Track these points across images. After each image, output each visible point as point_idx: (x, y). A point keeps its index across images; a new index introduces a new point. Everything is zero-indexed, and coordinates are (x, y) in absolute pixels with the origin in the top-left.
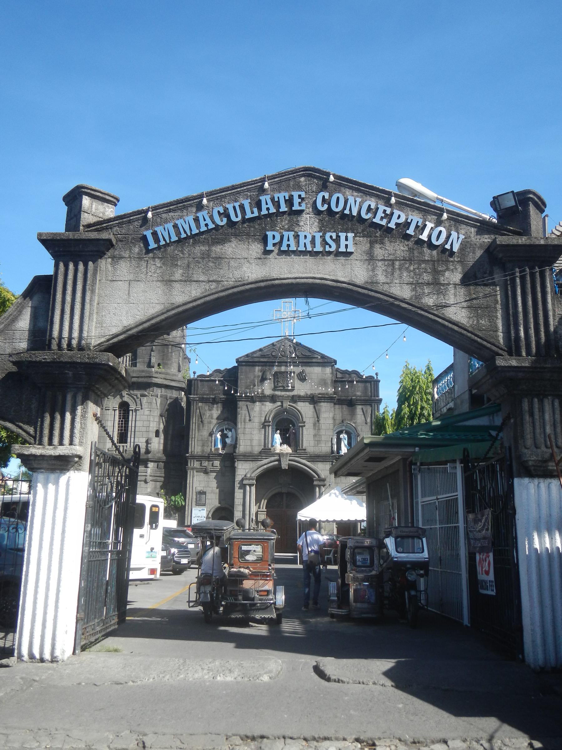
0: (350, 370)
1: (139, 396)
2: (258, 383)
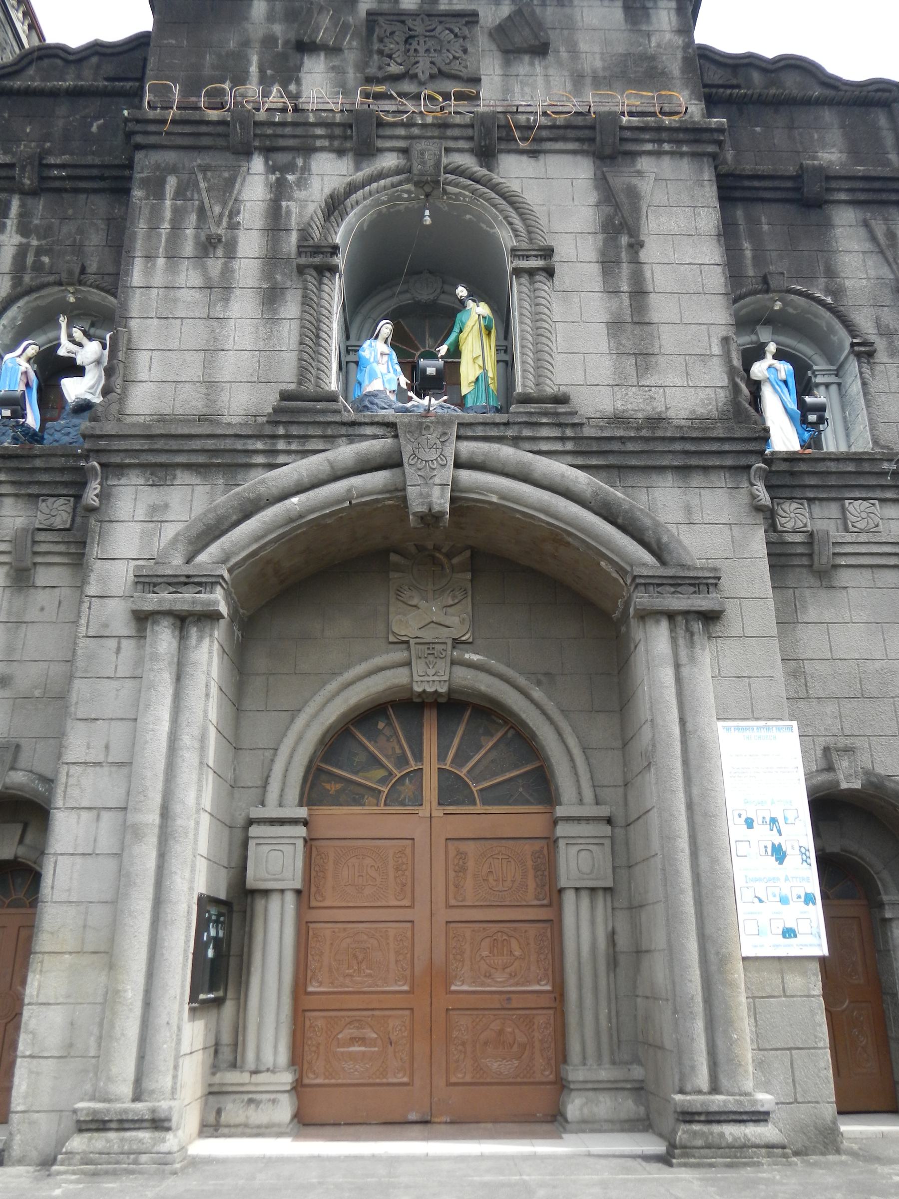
0: (769, 52)
2: (262, 71)
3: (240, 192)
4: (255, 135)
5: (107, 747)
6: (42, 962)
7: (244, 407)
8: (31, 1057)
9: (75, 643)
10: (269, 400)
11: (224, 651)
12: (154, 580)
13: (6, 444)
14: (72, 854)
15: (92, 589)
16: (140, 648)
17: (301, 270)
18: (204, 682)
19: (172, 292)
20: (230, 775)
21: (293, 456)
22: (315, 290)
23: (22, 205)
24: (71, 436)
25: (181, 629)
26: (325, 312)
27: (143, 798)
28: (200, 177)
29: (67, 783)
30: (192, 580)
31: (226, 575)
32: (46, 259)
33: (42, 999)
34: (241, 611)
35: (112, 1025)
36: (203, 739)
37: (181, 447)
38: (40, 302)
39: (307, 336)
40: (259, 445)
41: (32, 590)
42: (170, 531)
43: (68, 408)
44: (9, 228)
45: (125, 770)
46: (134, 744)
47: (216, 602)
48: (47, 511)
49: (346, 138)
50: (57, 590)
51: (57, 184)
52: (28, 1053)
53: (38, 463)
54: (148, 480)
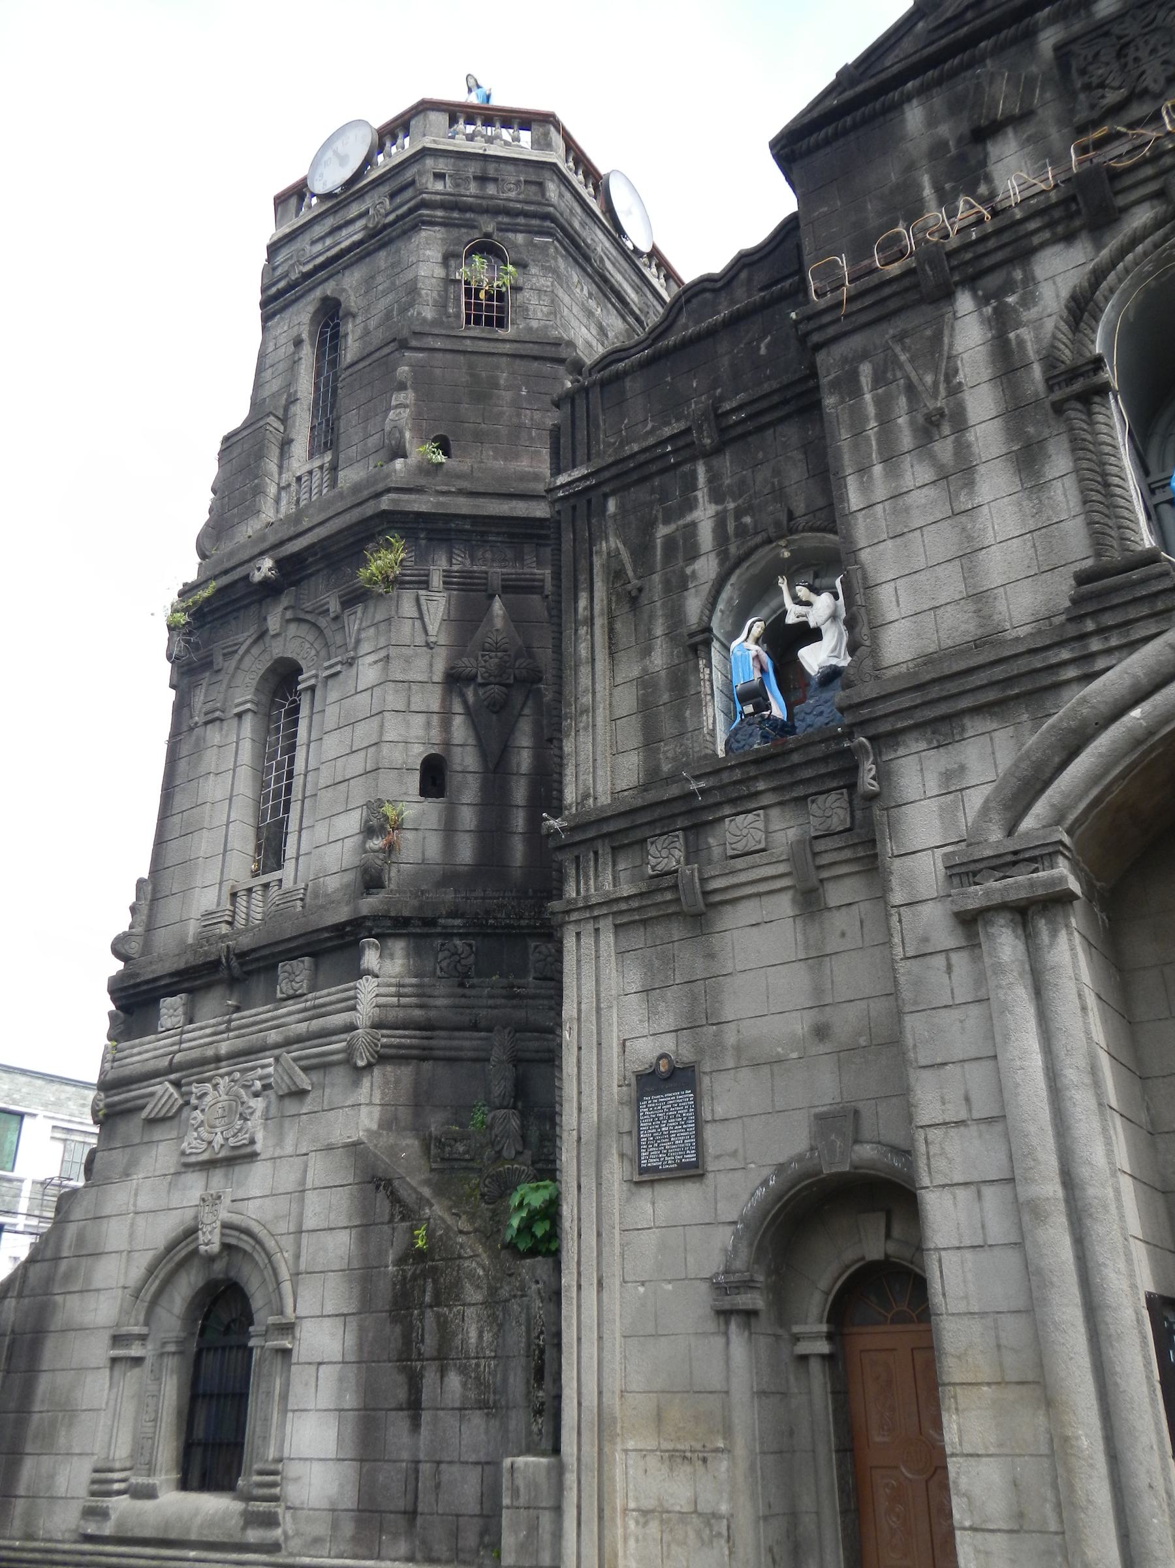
1: (334, 606)
3: (951, 345)
4: (952, 269)
5: (967, 1099)
6: (955, 1397)
7: (1030, 611)
8: (973, 1529)
9: (894, 970)
10: (1062, 589)
11: (1090, 944)
12: (972, 867)
13: (756, 746)
14: (958, 1248)
15: (897, 897)
16: (977, 959)
17: (1058, 408)
18: (1074, 991)
19: (900, 502)
20: (1143, 1118)
21: (1117, 654)
22: (1085, 427)
23: (709, 469)
24: (825, 715)
25: (1025, 926)
26: (1107, 449)
27: (1032, 1163)
28: (898, 349)
29: (928, 1153)
30: (1021, 856)
31: (1066, 839)
32: (747, 520)
33: (968, 1449)
34: (1098, 884)
35: (1071, 1488)
36: (1094, 1070)
37: (961, 689)
38: (752, 571)
39: (1092, 490)
40: (1065, 655)
41: (826, 914)
42: (975, 800)
43: (813, 683)
44: (701, 500)
45: (998, 1128)
46: (1001, 1091)
47: (1062, 879)
48: (819, 813)
49: (1071, 216)
50: (854, 907)
51: (739, 430)
52: (967, 1524)
53: (796, 758)
54: (930, 742)
